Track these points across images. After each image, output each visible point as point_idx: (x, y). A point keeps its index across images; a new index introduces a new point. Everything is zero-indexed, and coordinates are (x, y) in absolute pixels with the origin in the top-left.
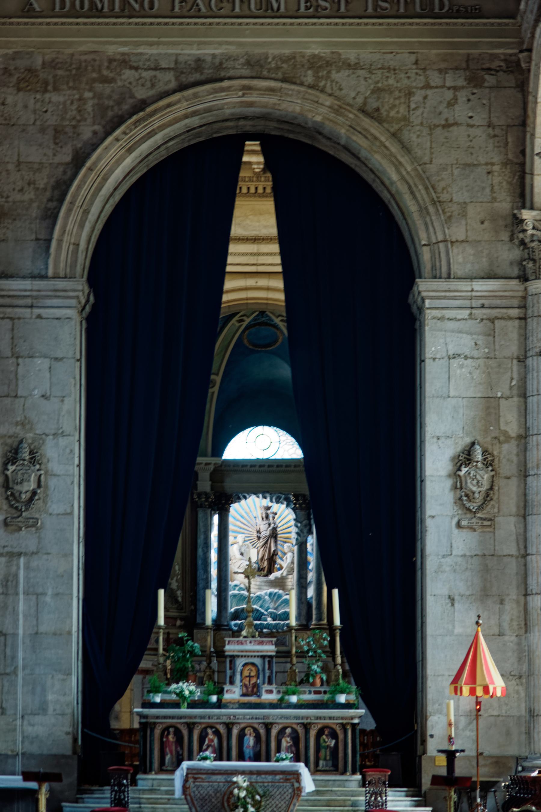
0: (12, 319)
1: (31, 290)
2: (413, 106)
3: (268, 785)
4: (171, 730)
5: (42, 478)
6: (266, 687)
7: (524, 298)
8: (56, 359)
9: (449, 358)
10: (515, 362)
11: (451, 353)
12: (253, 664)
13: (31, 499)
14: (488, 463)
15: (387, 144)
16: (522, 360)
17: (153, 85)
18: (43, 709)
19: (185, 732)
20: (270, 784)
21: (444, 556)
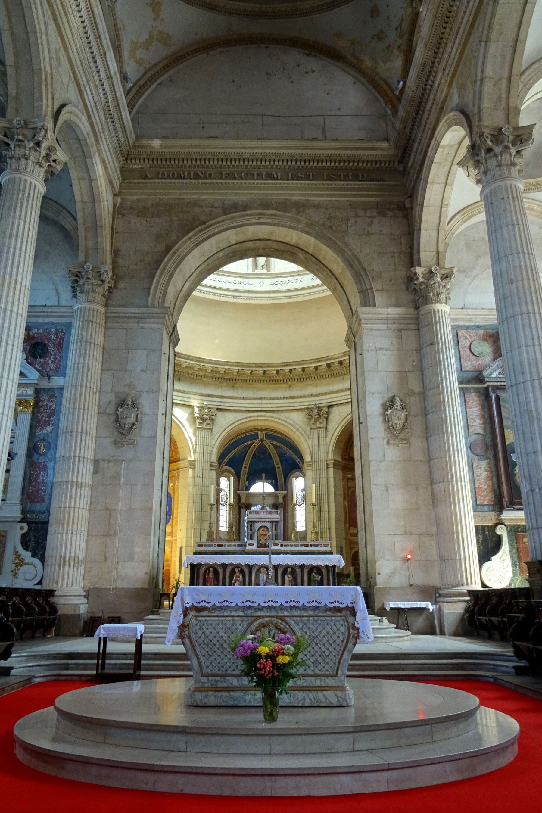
0: (126, 329)
1: (138, 313)
2: (350, 225)
3: (309, 621)
4: (211, 569)
5: (139, 416)
7: (417, 319)
8: (152, 351)
9: (377, 350)
10: (414, 352)
11: (378, 347)
12: (266, 527)
13: (131, 428)
14: (403, 408)
15: (337, 242)
16: (419, 350)
17: (210, 215)
18: (131, 557)
19: (221, 571)
20: (311, 618)
21: (380, 461)
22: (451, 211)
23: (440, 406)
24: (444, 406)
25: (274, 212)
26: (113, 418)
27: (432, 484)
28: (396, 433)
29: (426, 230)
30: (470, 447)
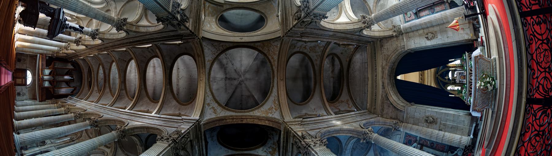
6: (464, 74)
22: (380, 29)
23: (425, 23)
24: (425, 22)
25: (384, 75)
26: (430, 124)
27: (444, 23)
28: (434, 36)
29: (384, 34)
30: (433, 13)
